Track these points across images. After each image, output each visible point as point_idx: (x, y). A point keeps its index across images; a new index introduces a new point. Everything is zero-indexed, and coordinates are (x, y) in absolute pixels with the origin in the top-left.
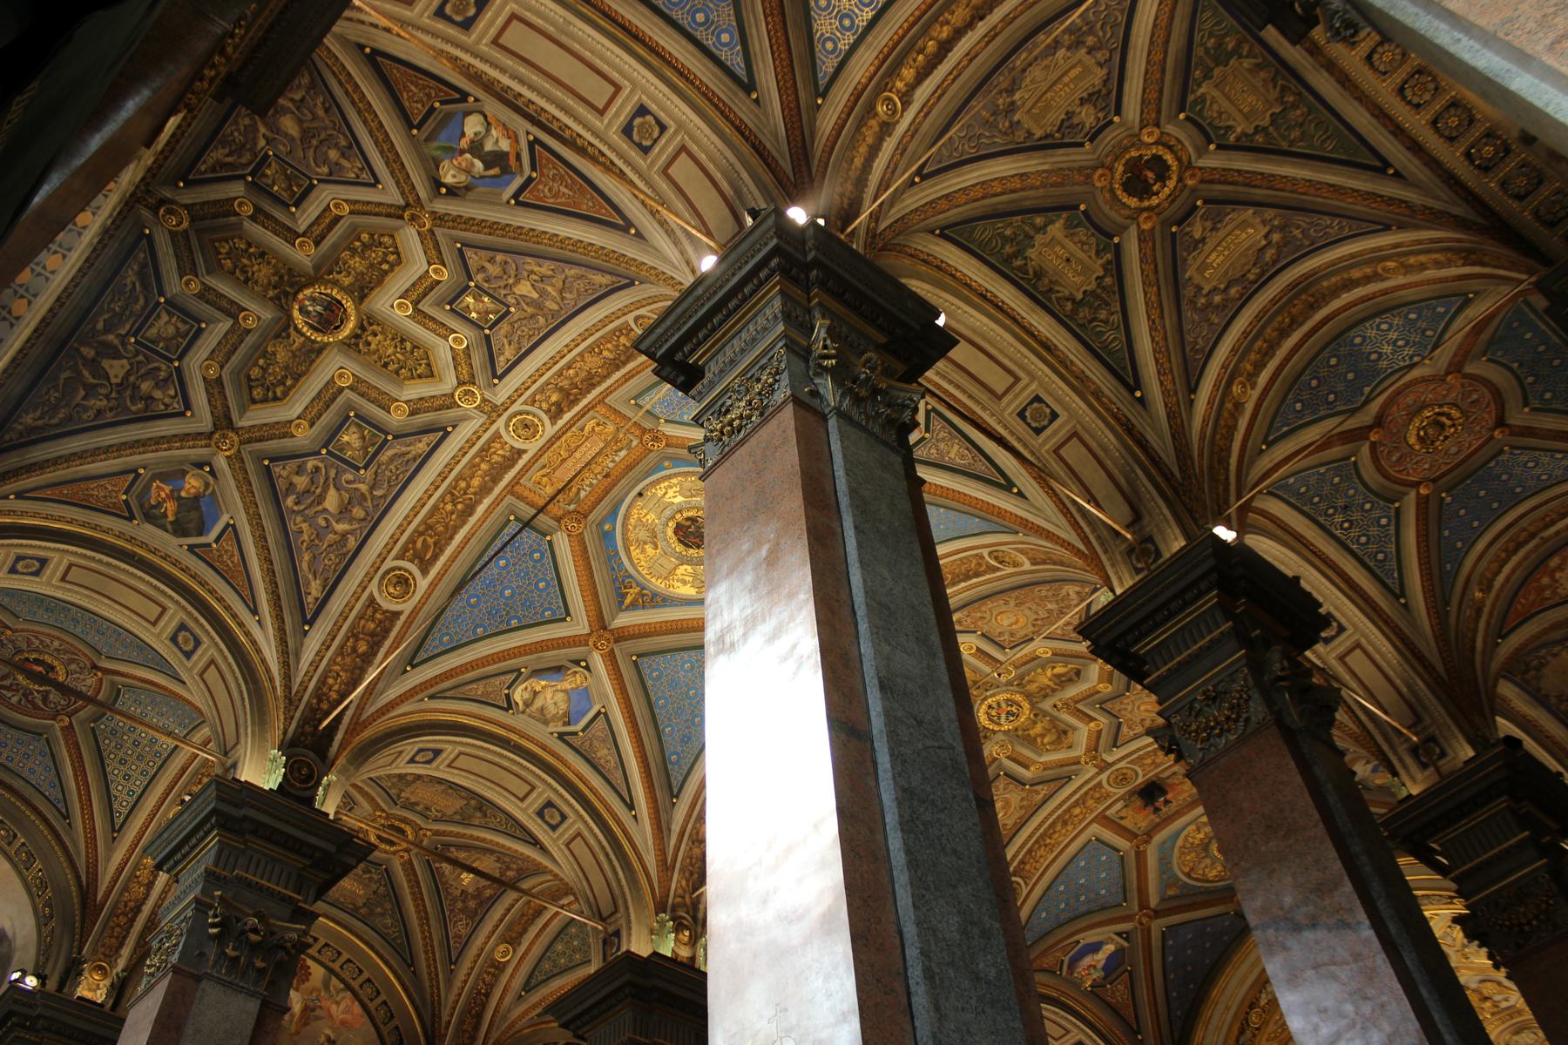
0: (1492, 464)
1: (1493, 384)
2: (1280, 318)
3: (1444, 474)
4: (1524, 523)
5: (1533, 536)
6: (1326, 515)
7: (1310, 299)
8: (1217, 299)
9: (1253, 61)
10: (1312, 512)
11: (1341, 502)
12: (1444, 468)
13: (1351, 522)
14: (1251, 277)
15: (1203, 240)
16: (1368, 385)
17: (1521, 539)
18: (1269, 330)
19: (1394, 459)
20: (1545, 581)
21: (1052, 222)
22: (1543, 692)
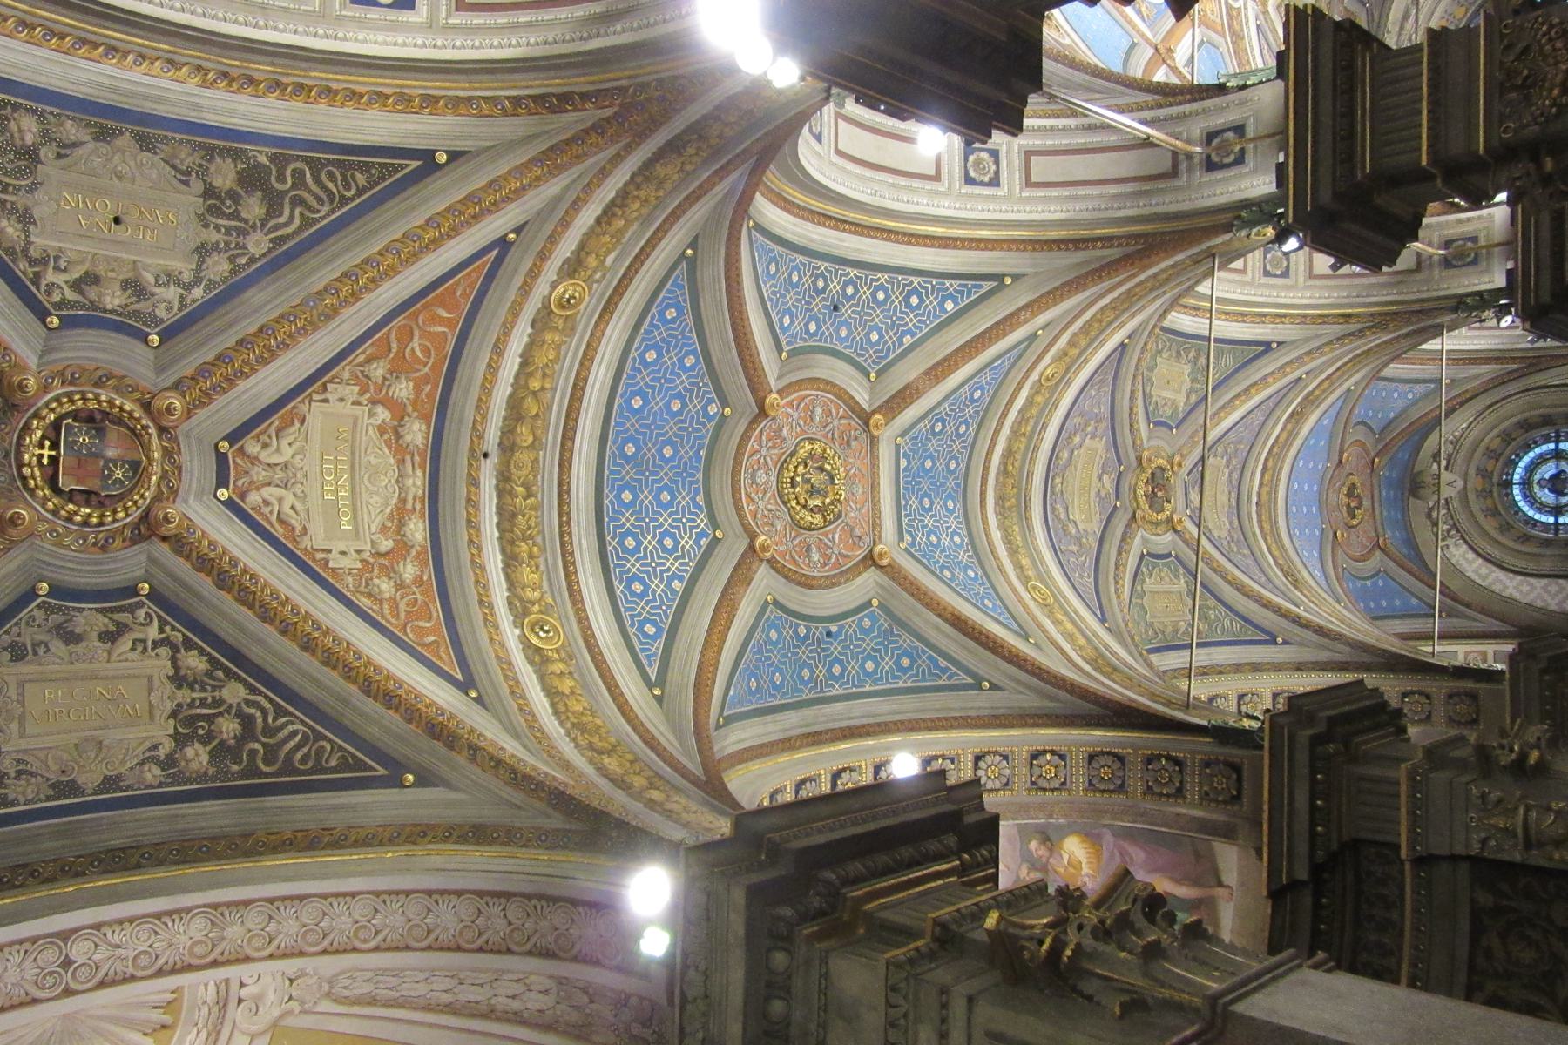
0: (700, 499)
1: (820, 587)
2: (1017, 464)
3: (745, 438)
4: (551, 457)
5: (508, 447)
6: (851, 282)
7: (1007, 504)
8: (1077, 439)
9: (1182, 630)
10: (872, 275)
11: (846, 310)
12: (752, 444)
13: (819, 292)
14: (1058, 480)
15: (1100, 478)
16: (905, 470)
17: (523, 430)
18: (1022, 447)
19: (819, 411)
20: (403, 390)
21: (1185, 404)
22: (125, 141)
